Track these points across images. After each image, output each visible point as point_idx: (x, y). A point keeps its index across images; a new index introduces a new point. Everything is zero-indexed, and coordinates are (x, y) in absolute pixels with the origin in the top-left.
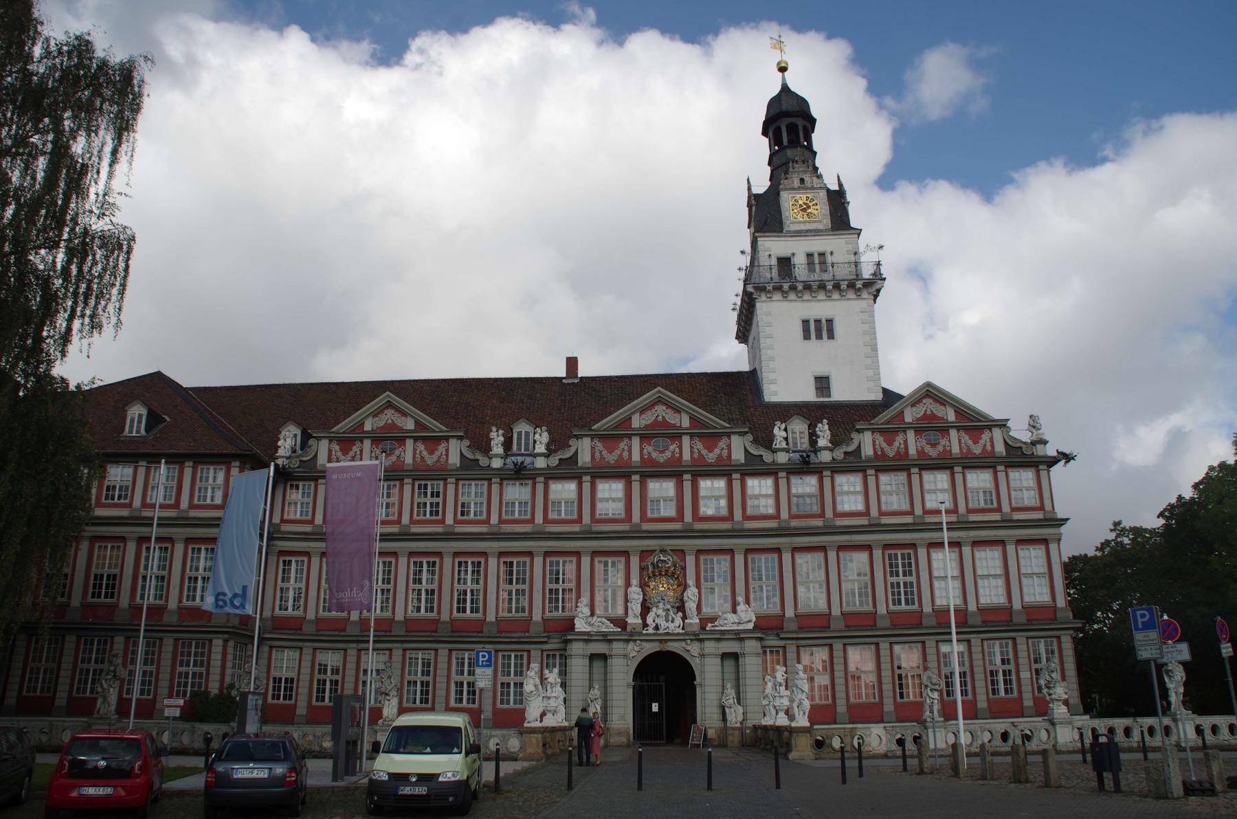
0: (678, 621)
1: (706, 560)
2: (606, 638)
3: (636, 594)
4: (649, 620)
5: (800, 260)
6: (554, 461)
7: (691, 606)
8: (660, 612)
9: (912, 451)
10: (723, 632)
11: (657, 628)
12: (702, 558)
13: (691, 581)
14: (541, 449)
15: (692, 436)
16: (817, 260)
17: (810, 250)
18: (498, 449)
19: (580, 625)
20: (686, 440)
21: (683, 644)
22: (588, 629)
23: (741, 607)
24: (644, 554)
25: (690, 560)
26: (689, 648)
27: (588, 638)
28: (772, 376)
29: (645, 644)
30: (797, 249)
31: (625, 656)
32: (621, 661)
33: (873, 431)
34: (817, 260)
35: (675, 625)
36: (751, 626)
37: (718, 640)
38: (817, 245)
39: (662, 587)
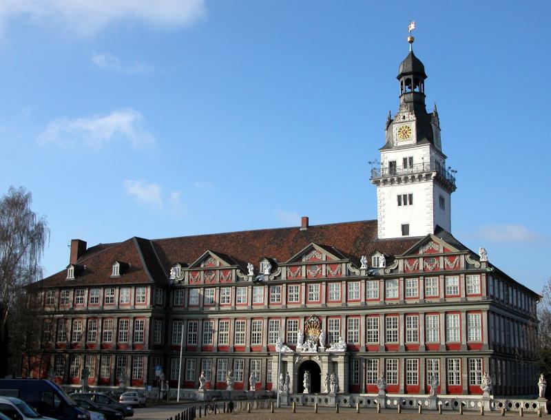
0: (315, 348)
5: (400, 164)
6: (272, 278)
9: (421, 268)
11: (307, 350)
14: (267, 272)
15: (326, 264)
16: (408, 162)
17: (405, 156)
18: (251, 273)
19: (278, 349)
20: (324, 266)
24: (306, 318)
25: (324, 320)
28: (383, 226)
30: (398, 156)
33: (404, 259)
34: (408, 162)
35: (313, 350)
38: (407, 153)
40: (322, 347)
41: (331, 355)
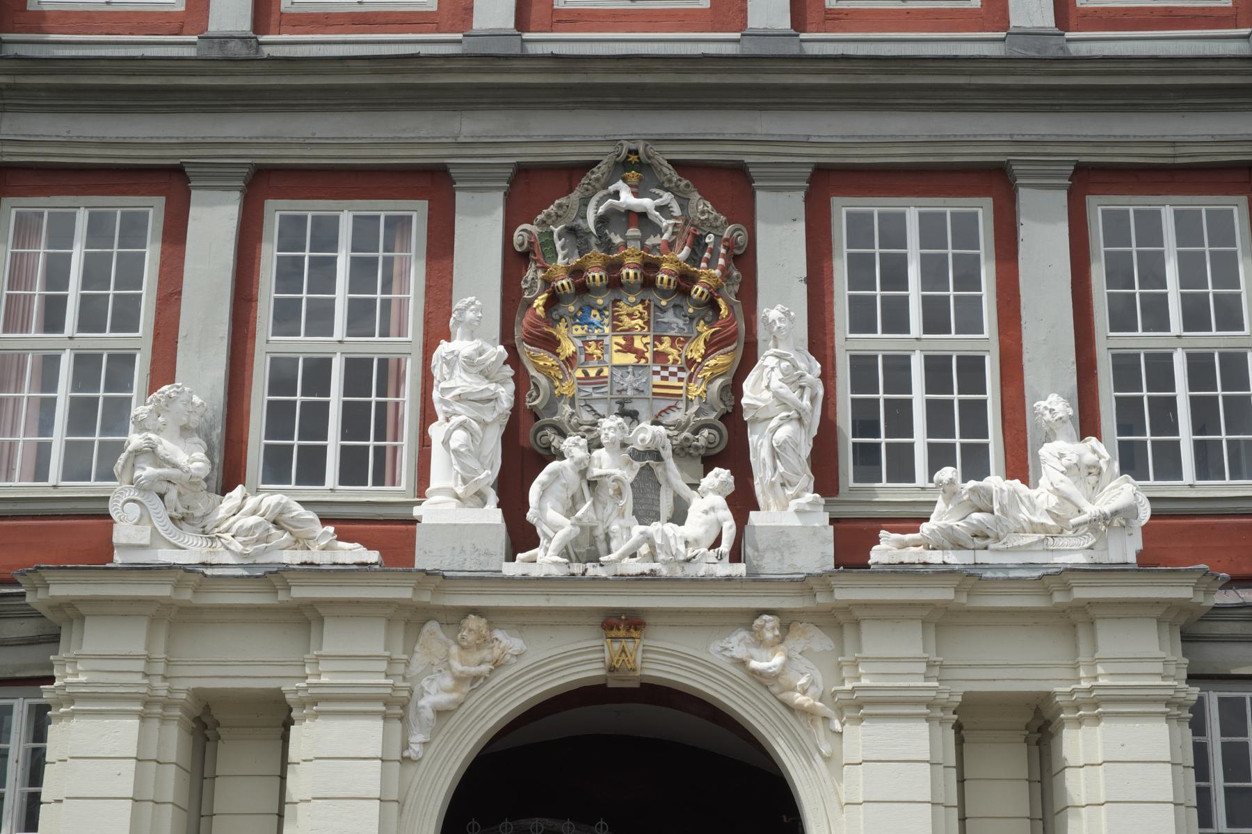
1: (859, 225)
2: (289, 604)
3: (468, 370)
4: (546, 503)
7: (778, 440)
8: (605, 463)
10: (969, 578)
11: (588, 547)
12: (842, 209)
13: (781, 309)
21: (737, 644)
22: (190, 550)
23: (1059, 454)
24: (531, 186)
26: (770, 662)
27: (184, 605)
29: (508, 642)
31: (395, 708)
32: (367, 735)
36: (1126, 549)
37: (940, 620)
39: (608, 346)
40: (792, 517)
41: (958, 605)
